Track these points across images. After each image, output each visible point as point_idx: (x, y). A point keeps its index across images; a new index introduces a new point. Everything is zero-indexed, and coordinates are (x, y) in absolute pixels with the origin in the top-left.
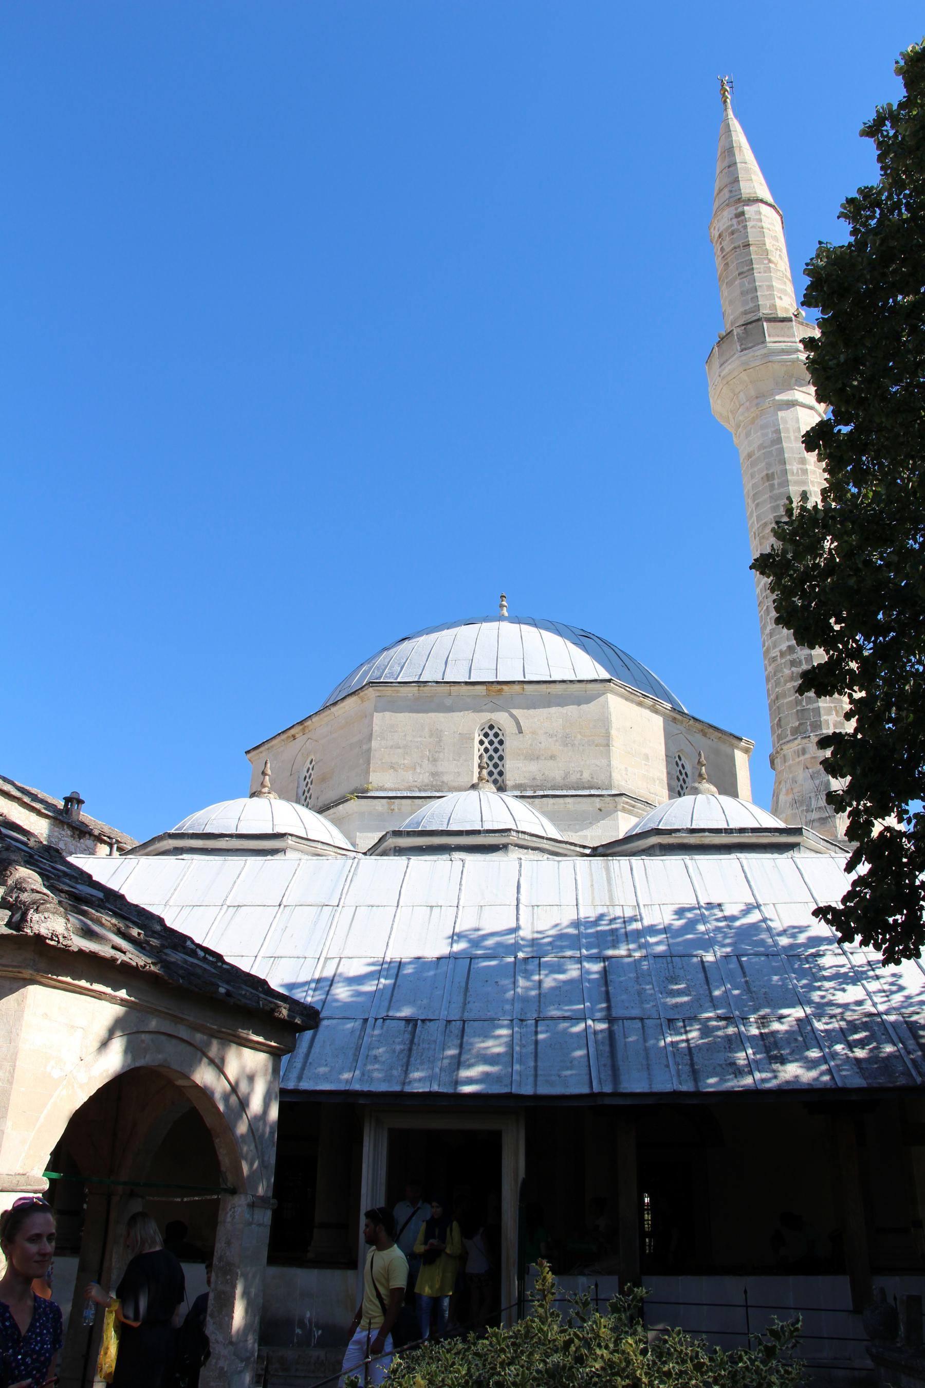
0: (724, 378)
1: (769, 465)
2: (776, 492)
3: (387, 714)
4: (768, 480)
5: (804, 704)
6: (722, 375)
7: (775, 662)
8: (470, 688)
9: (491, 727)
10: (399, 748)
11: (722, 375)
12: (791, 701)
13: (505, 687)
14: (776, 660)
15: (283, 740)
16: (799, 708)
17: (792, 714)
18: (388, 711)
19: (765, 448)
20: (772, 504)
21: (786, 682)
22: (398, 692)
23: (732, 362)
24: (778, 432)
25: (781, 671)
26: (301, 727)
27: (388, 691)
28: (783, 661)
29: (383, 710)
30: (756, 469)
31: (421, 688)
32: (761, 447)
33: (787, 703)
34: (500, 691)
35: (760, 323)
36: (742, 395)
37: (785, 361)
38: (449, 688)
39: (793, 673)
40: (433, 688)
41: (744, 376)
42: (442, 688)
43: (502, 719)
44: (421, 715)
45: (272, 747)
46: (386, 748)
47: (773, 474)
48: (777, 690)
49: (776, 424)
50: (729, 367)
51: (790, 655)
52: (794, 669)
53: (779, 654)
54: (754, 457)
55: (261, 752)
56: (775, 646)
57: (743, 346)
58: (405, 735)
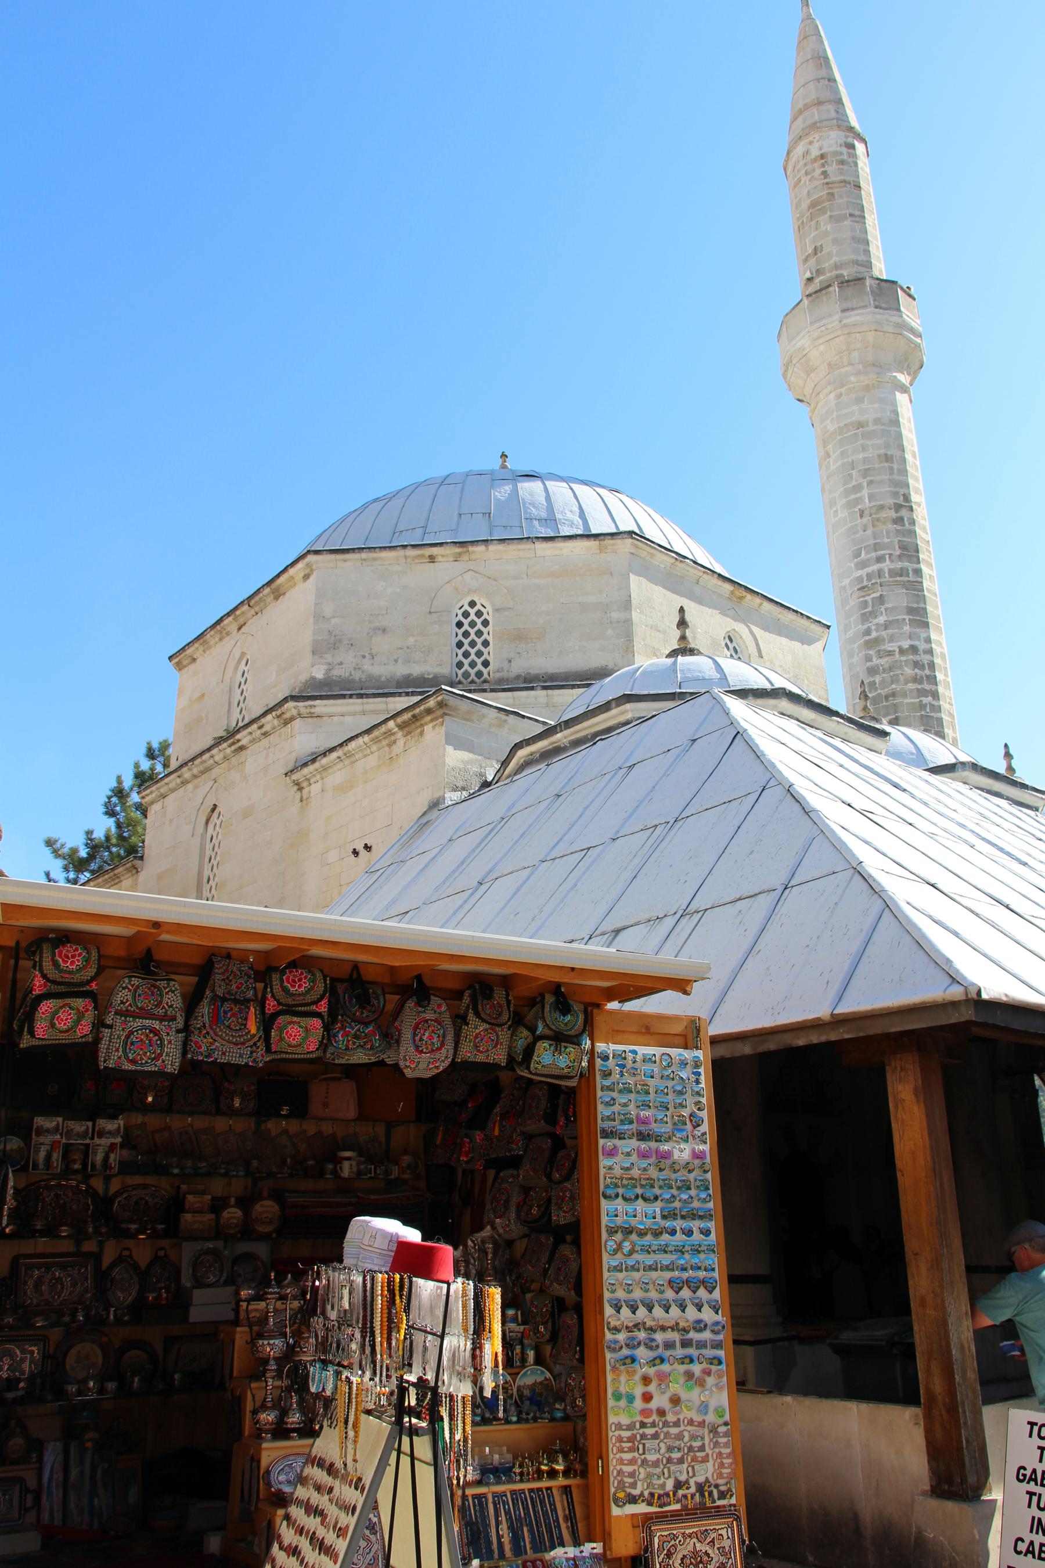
0: (845, 326)
1: (887, 446)
2: (895, 477)
3: (644, 581)
4: (887, 461)
5: (928, 710)
6: (844, 321)
7: (892, 657)
8: (720, 583)
9: (731, 640)
10: (659, 631)
11: (844, 321)
12: (913, 703)
13: (749, 596)
14: (894, 655)
15: (406, 557)
16: (923, 713)
17: (914, 716)
18: (644, 577)
19: (883, 424)
20: (892, 489)
21: (907, 682)
22: (652, 555)
23: (863, 314)
24: (896, 413)
25: (901, 668)
26: (458, 550)
27: (644, 551)
28: (903, 658)
29: (639, 574)
30: (870, 443)
31: (678, 563)
32: (877, 421)
33: (907, 703)
34: (741, 598)
35: (894, 286)
36: (855, 355)
37: (911, 341)
38: (701, 574)
39: (916, 675)
40: (688, 568)
41: (871, 337)
42: (695, 572)
43: (741, 629)
44: (675, 596)
45: (374, 559)
46: (647, 626)
47: (892, 456)
48: (894, 686)
49: (894, 404)
50: (858, 318)
51: (913, 654)
52: (917, 670)
53: (897, 650)
54: (866, 429)
55: (345, 561)
56: (892, 639)
57: (877, 303)
58: (663, 617)
